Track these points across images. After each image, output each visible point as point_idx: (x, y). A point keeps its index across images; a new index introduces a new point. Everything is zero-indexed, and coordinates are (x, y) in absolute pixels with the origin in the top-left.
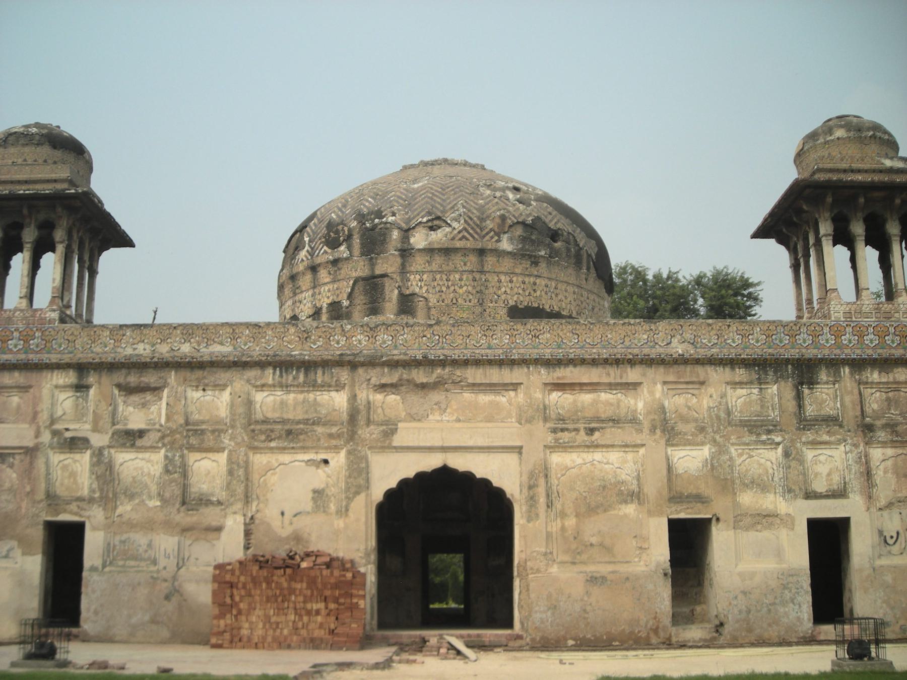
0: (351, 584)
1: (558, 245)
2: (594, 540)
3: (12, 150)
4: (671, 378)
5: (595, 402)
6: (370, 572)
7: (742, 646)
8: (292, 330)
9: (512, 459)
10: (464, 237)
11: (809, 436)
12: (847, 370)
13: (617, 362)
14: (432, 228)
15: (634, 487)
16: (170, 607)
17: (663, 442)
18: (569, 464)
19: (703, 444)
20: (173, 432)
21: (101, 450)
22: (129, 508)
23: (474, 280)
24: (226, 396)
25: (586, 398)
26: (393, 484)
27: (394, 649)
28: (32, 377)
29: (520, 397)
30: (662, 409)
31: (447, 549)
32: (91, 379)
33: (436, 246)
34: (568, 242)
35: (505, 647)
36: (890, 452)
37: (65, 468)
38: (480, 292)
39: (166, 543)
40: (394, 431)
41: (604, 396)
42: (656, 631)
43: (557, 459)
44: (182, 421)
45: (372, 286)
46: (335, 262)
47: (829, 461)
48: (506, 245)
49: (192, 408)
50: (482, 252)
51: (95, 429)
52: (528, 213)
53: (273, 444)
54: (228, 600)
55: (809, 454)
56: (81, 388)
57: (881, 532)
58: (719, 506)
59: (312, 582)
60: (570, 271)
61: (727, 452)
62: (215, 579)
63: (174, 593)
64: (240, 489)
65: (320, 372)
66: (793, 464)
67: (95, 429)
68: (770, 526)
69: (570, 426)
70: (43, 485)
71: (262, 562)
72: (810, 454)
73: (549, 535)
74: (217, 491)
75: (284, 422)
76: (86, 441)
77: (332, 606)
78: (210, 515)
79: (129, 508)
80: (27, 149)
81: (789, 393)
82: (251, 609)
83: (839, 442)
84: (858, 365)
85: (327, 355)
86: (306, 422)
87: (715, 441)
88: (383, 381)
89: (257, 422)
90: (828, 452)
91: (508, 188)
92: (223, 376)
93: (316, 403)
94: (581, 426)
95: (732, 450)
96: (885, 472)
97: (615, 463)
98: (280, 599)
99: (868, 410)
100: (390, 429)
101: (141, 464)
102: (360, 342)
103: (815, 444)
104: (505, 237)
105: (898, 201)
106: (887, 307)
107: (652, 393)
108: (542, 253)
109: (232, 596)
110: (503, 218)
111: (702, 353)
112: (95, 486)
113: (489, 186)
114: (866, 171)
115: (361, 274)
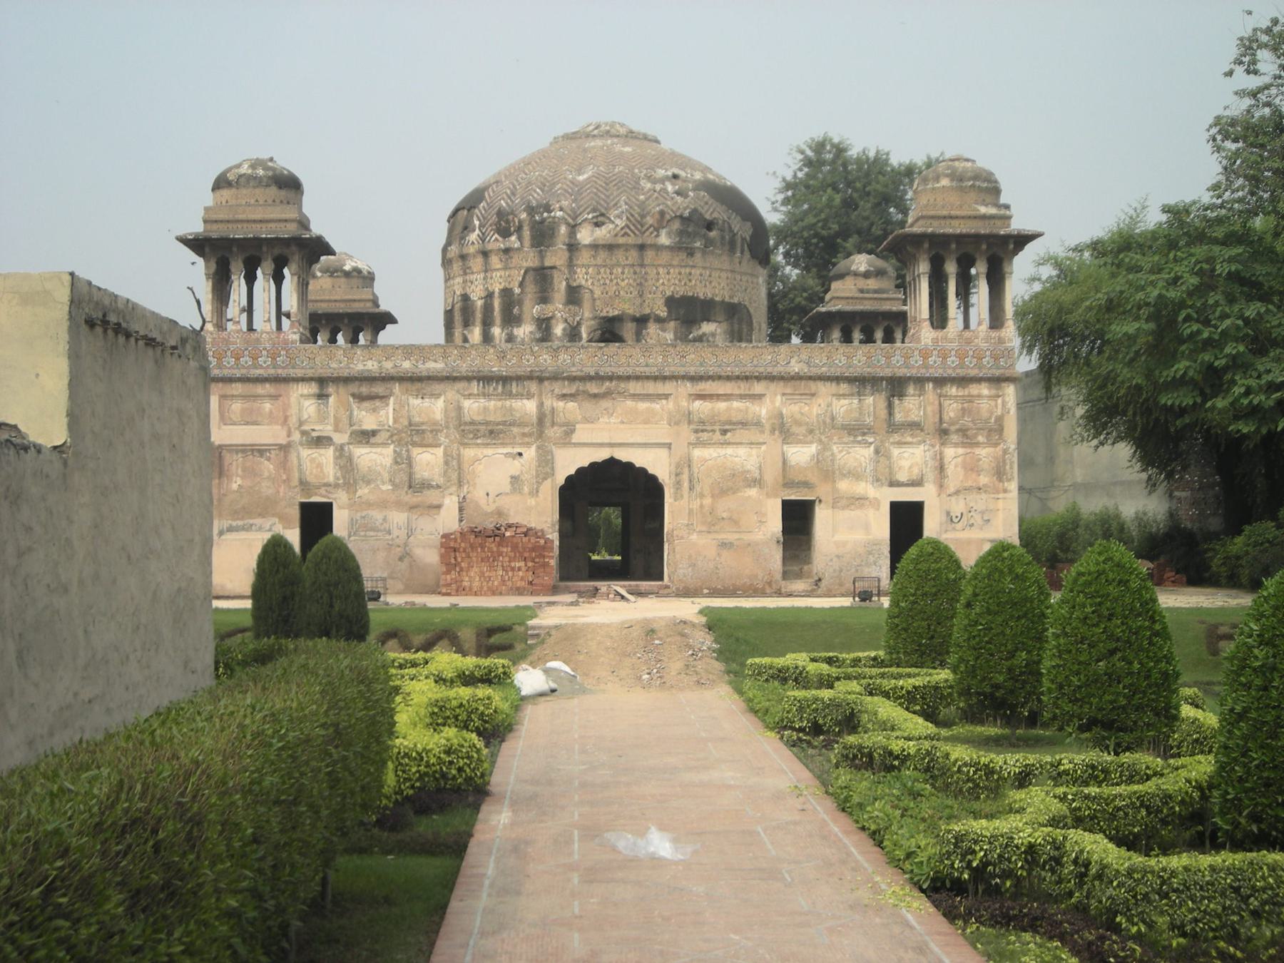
0: (544, 548)
1: (713, 234)
2: (725, 515)
3: (244, 191)
4: (788, 391)
5: (728, 409)
6: (554, 537)
7: (835, 596)
8: (492, 351)
9: (663, 453)
10: (626, 234)
11: (896, 437)
12: (931, 385)
13: (747, 378)
14: (597, 225)
15: (757, 475)
16: (403, 566)
17: (780, 441)
18: (707, 457)
19: (811, 442)
20: (400, 432)
21: (342, 446)
22: (366, 491)
23: (635, 273)
24: (440, 403)
25: (722, 405)
26: (572, 472)
27: (575, 595)
28: (283, 386)
29: (670, 405)
30: (781, 414)
31: (613, 522)
32: (330, 389)
33: (601, 242)
34: (722, 230)
35: (657, 594)
36: (961, 451)
37: (313, 460)
38: (641, 284)
39: (398, 518)
40: (573, 431)
41: (736, 404)
42: (770, 584)
43: (697, 453)
44: (406, 423)
45: (542, 276)
46: (507, 251)
47: (911, 457)
48: (664, 240)
49: (414, 412)
50: (642, 247)
51: (336, 430)
52: (683, 205)
53: (479, 441)
54: (453, 561)
55: (896, 452)
56: (322, 396)
57: (948, 513)
58: (821, 491)
59: (515, 548)
60: (725, 257)
61: (831, 450)
62: (442, 545)
63: (405, 555)
64: (454, 476)
65: (514, 384)
66: (882, 459)
67: (336, 430)
68: (862, 506)
69: (709, 428)
70: (297, 475)
71: (476, 533)
72: (896, 452)
73: (691, 512)
74: (436, 477)
75: (487, 423)
76: (329, 439)
77: (530, 564)
78: (431, 496)
79: (366, 491)
80: (257, 191)
81: (882, 404)
82: (470, 567)
83: (919, 443)
84: (940, 382)
85: (520, 372)
86: (504, 423)
87: (820, 441)
88: (564, 392)
89: (466, 424)
90: (911, 450)
91: (667, 178)
92: (437, 387)
93: (511, 409)
94: (717, 428)
95: (834, 448)
96: (956, 466)
97: (743, 456)
98: (491, 559)
99: (946, 418)
100: (570, 430)
101: (375, 456)
102: (545, 360)
103: (900, 444)
104: (663, 232)
105: (984, 247)
106: (967, 334)
107: (773, 402)
108: (698, 244)
109: (455, 558)
110: (662, 213)
111: (815, 371)
112: (339, 474)
113: (649, 178)
114: (963, 218)
115: (529, 264)
